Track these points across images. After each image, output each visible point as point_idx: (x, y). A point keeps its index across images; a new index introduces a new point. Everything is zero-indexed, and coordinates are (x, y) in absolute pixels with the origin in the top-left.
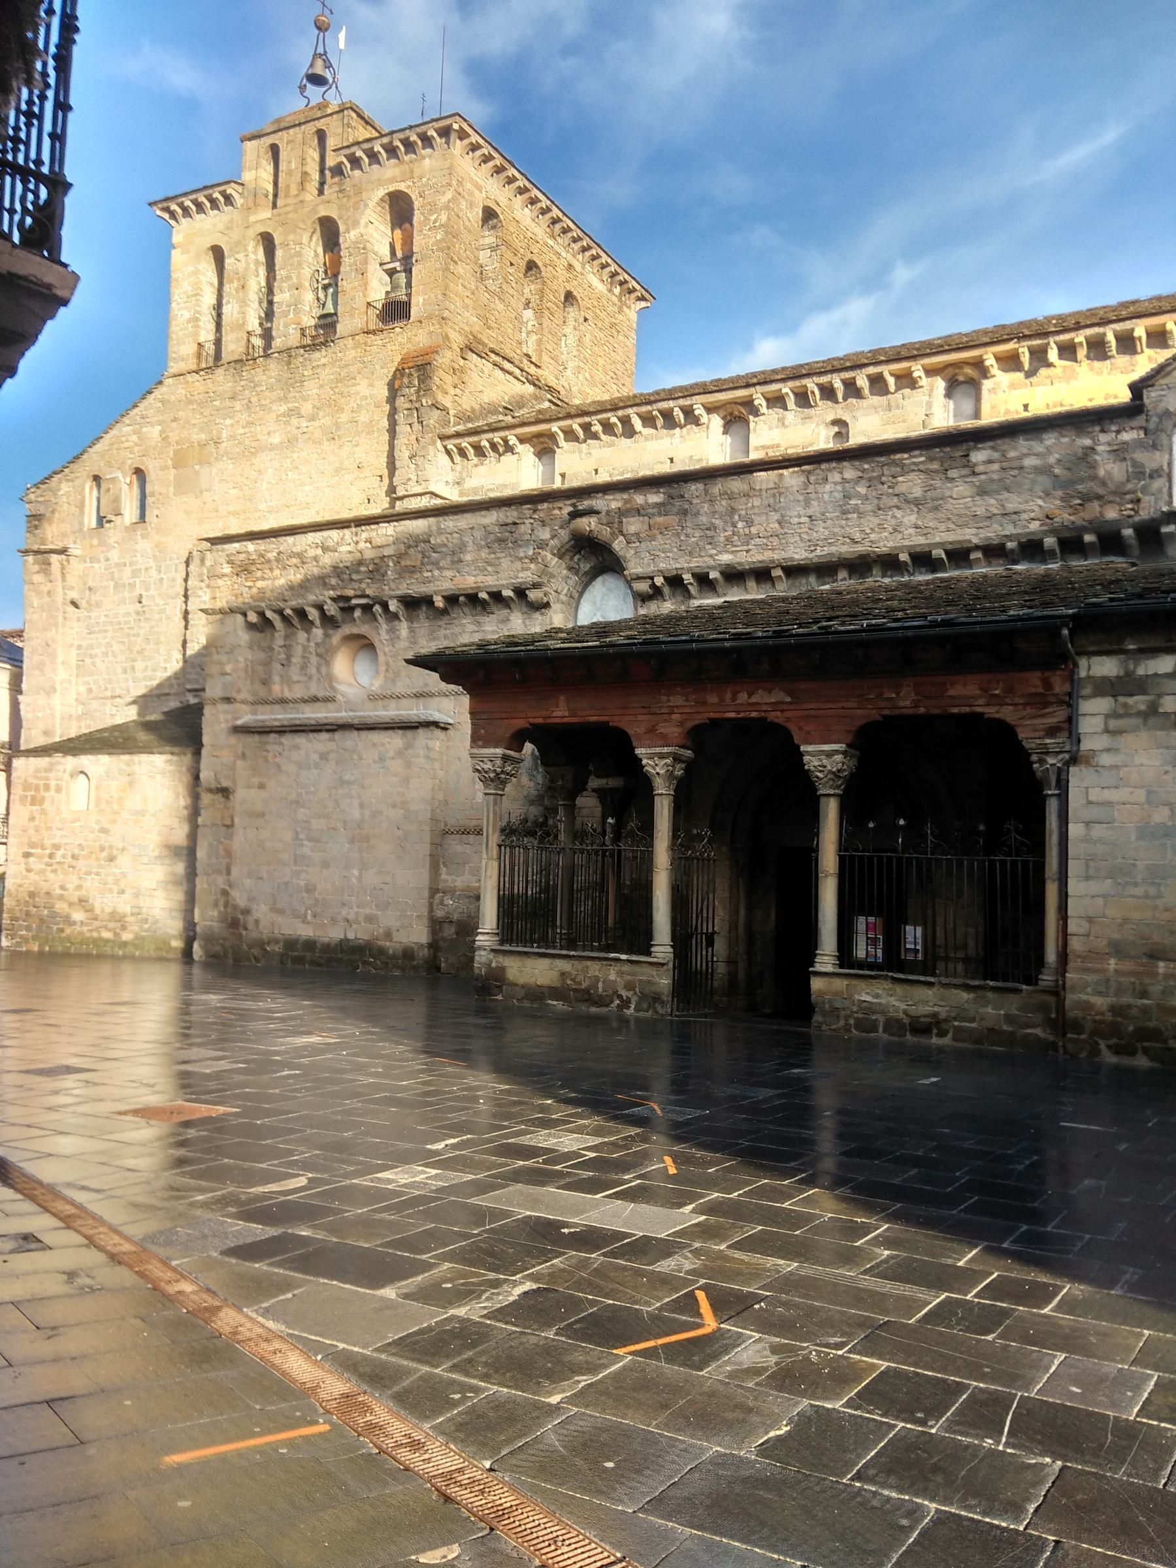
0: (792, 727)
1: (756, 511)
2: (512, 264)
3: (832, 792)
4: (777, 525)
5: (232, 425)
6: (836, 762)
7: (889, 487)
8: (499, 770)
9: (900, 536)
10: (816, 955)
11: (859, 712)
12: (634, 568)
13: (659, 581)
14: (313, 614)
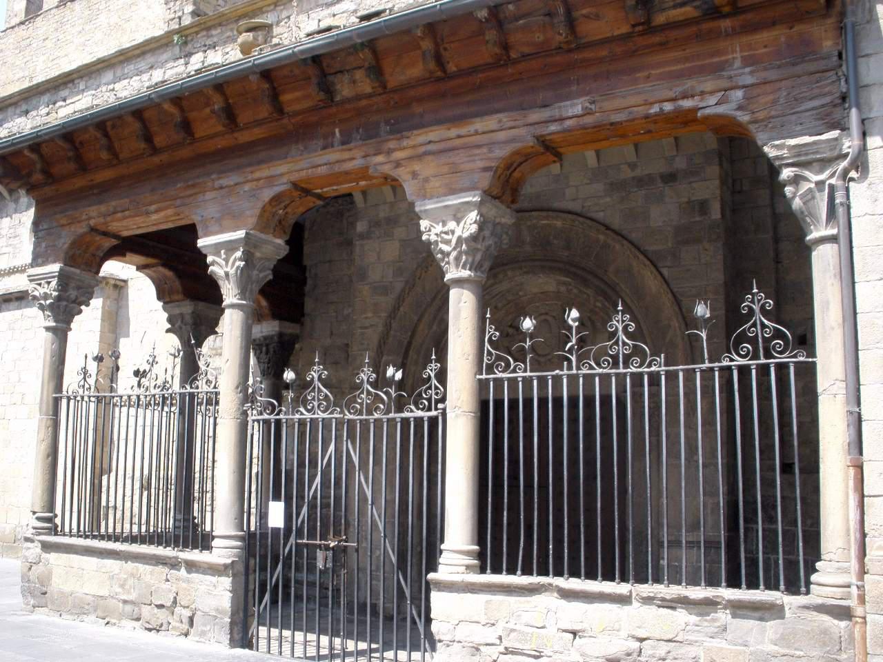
0: (403, 174)
3: (466, 273)
6: (469, 225)
8: (55, 294)
10: (441, 552)
11: (502, 136)
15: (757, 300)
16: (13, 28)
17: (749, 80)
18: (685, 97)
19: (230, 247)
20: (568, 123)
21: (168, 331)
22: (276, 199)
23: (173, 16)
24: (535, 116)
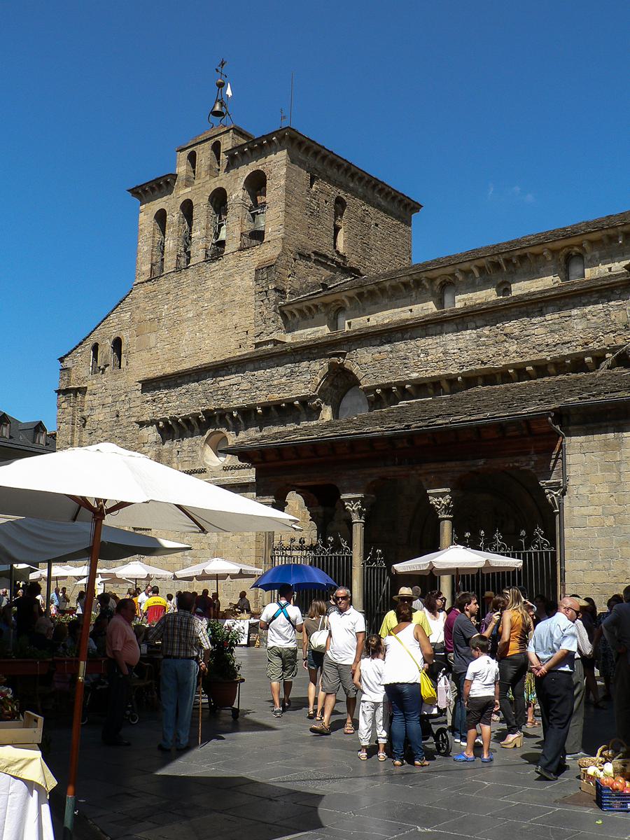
1: (430, 347)
2: (326, 202)
4: (442, 355)
5: (168, 309)
7: (501, 330)
9: (508, 358)
12: (365, 384)
13: (379, 391)
14: (193, 422)
15: (539, 531)
16: (143, 283)
17: (536, 459)
18: (516, 462)
19: (355, 500)
20: (480, 467)
21: (310, 520)
22: (372, 483)
23: (261, 290)
24: (468, 463)
